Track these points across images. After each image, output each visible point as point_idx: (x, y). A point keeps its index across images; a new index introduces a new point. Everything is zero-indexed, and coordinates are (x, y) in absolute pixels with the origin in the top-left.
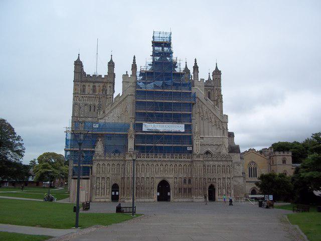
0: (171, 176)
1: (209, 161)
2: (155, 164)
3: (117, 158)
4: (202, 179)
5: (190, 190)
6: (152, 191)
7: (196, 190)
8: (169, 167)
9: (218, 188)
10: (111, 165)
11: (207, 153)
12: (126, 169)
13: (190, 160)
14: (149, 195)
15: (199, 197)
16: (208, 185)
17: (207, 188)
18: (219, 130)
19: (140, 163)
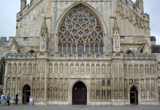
0: (88, 77)
1: (131, 60)
2: (69, 63)
3: (29, 58)
4: (123, 80)
5: (109, 92)
6: (66, 93)
7: (116, 93)
8: (85, 67)
9: (142, 90)
10: (22, 64)
11: (129, 52)
12: (36, 68)
13: (109, 58)
14: (64, 98)
15: (118, 100)
16: (130, 86)
17: (129, 90)
18: (140, 29)
19: (53, 63)
